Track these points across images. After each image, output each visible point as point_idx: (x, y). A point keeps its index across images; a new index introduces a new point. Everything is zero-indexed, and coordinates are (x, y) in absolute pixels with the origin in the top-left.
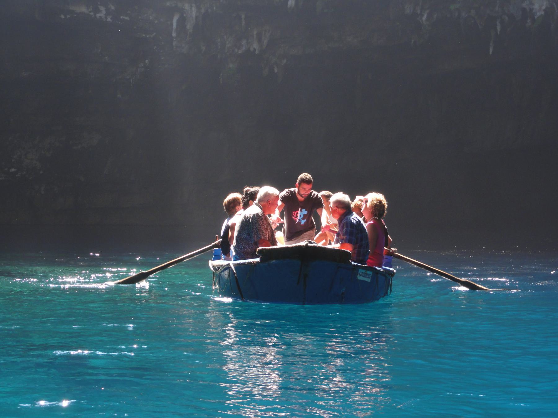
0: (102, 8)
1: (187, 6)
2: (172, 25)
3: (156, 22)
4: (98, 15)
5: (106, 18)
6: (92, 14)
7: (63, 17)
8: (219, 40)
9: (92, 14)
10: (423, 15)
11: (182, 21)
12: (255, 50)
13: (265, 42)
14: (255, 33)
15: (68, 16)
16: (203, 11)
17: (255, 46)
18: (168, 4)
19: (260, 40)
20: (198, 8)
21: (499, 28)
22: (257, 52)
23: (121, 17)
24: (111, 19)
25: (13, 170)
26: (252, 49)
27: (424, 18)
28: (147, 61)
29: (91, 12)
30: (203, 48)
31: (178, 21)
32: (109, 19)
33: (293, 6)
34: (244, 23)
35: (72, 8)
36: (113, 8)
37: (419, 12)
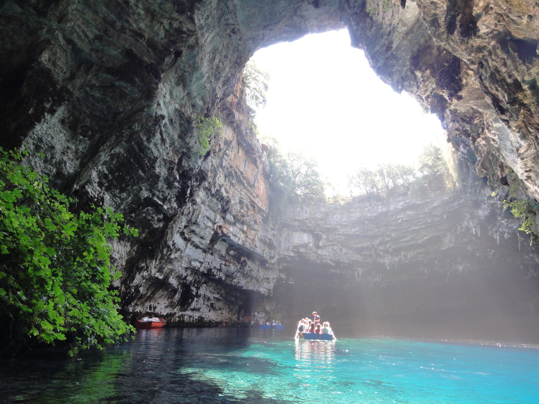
11: (358, 273)
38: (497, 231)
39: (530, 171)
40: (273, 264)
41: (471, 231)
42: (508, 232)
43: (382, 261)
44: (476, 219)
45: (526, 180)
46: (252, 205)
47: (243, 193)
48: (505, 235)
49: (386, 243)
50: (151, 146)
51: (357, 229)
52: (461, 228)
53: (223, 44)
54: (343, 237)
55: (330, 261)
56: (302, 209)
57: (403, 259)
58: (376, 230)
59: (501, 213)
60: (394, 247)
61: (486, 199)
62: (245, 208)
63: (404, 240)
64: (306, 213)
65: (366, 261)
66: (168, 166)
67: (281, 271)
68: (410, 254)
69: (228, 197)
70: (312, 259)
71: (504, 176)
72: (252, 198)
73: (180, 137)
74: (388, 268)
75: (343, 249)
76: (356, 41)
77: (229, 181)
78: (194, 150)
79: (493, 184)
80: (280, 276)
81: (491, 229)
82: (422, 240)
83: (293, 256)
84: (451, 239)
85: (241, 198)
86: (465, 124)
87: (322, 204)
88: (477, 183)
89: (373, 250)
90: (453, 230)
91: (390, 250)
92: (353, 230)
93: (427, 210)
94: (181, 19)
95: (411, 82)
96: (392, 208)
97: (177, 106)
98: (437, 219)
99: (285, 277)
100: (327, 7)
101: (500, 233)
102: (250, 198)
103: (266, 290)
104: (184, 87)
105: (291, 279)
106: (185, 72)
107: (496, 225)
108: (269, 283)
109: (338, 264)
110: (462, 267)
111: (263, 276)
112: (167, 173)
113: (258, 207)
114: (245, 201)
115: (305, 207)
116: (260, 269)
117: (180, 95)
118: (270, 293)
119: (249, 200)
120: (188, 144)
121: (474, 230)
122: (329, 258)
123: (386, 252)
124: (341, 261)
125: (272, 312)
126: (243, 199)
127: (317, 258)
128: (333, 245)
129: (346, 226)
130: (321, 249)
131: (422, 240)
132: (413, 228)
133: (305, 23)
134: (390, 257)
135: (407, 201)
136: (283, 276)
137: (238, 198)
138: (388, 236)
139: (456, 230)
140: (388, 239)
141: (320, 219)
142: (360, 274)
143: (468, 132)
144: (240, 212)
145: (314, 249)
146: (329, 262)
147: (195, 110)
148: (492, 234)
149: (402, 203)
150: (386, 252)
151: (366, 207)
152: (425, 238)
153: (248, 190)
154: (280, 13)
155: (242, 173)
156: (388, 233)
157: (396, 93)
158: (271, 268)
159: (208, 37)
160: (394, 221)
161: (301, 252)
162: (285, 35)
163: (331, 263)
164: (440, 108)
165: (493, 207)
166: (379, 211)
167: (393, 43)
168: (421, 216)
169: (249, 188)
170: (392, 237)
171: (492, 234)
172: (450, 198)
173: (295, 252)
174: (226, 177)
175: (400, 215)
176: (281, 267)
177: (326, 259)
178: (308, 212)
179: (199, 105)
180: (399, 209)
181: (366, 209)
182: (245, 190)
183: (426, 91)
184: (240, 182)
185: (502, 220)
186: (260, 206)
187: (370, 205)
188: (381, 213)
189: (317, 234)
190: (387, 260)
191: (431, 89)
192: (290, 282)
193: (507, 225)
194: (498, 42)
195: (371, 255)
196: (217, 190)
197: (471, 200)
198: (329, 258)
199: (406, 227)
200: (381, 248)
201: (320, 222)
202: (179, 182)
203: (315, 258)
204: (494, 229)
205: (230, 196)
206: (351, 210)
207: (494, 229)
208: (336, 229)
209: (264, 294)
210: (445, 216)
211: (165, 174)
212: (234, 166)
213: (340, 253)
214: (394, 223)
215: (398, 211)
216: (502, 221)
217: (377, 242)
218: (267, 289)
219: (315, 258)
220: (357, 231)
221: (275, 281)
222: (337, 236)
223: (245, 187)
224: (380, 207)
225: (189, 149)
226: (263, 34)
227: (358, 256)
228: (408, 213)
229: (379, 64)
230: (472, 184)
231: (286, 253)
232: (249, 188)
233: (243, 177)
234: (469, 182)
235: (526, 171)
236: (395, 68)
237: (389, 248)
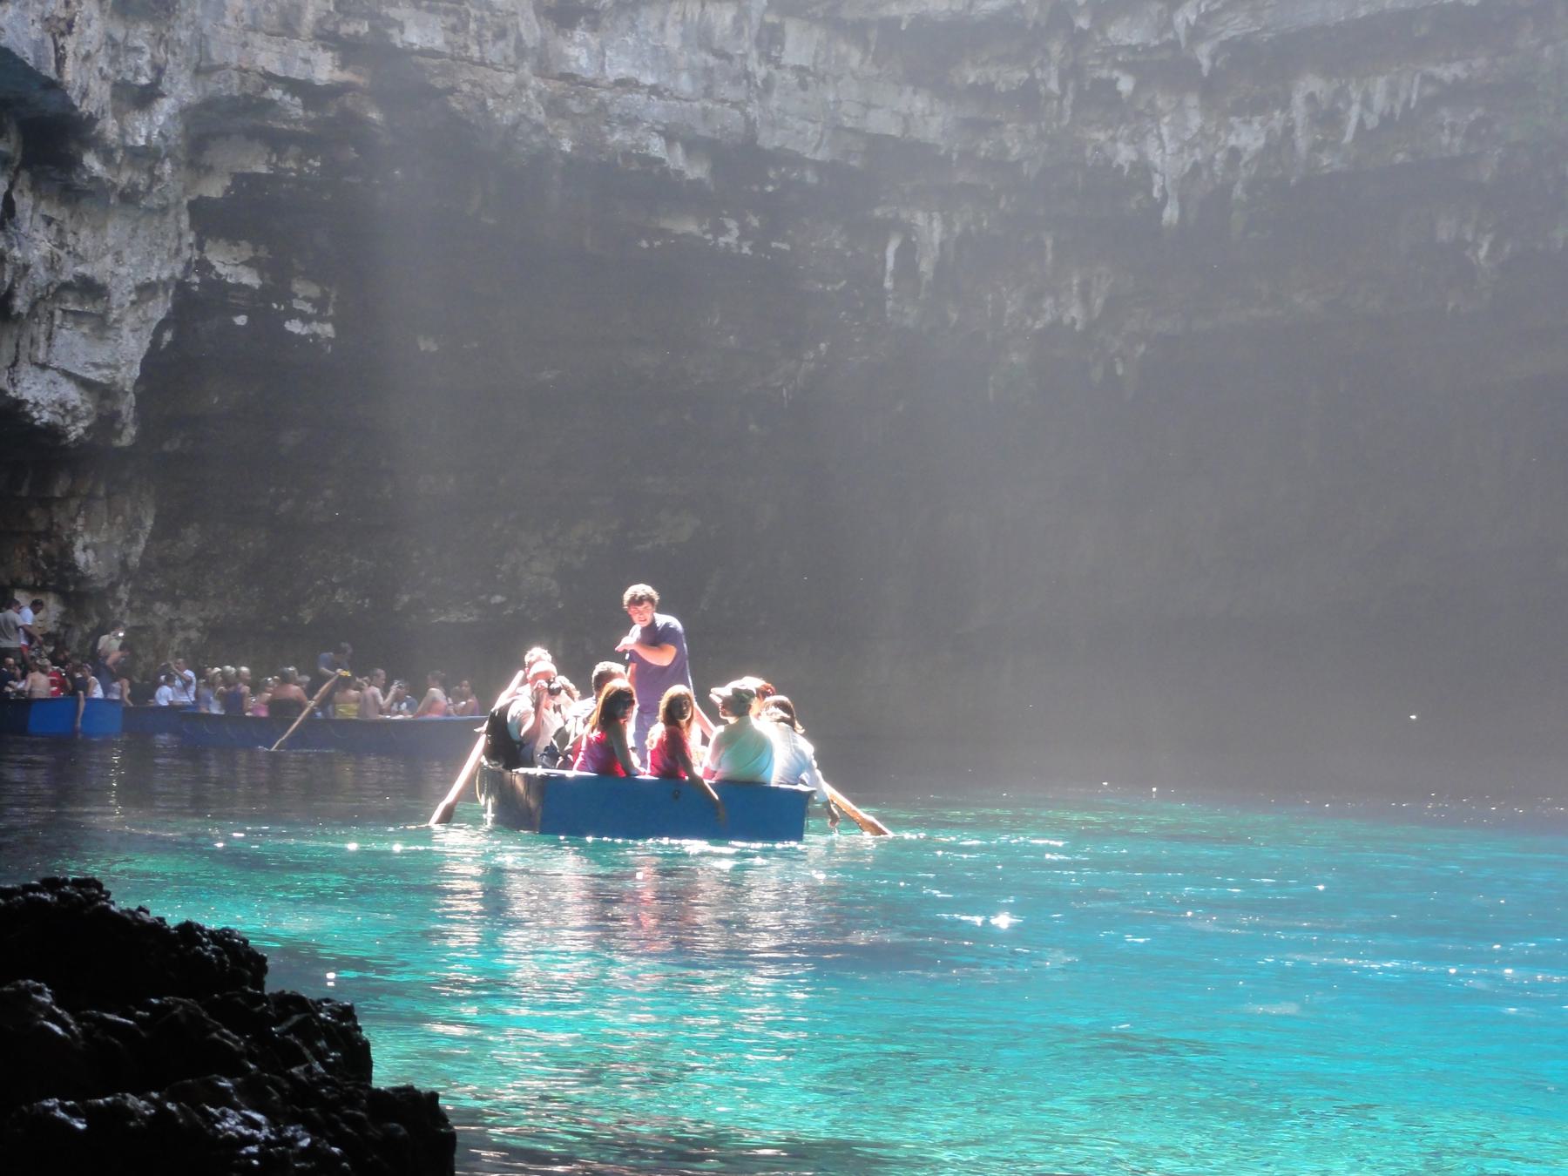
0: (732, 224)
1: (920, 218)
2: (884, 261)
3: (849, 254)
4: (722, 240)
5: (740, 248)
6: (709, 237)
7: (644, 244)
8: (990, 297)
9: (709, 237)
10: (1480, 246)
11: (908, 252)
12: (1074, 321)
13: (1099, 302)
14: (1075, 281)
15: (657, 243)
16: (957, 229)
17: (1075, 312)
18: (878, 212)
19: (1085, 298)
20: (948, 223)
22: (1078, 327)
23: (774, 244)
24: (751, 248)
25: (498, 599)
26: (1067, 320)
27: (1482, 253)
28: (823, 346)
29: (705, 233)
30: (954, 316)
31: (898, 254)
32: (746, 250)
33: (1175, 222)
34: (1050, 257)
35: (666, 224)
36: (755, 222)
37: (1469, 237)
40: (146, 157)
43: (1125, 154)
55: (669, 136)
57: (1302, 143)
60: (1236, 25)
65: (985, 147)
67: (210, 221)
68: (1374, 96)
70: (507, 116)
74: (1171, 213)
75: (792, 29)
80: (204, 266)
83: (334, 91)
89: (1056, 48)
91: (1203, 53)
99: (250, 278)
103: (73, 395)
105: (304, 291)
108: (102, 326)
109: (740, 162)
111: (52, 264)
116: (24, 202)
118: (107, 422)
122: (657, 108)
124: (769, 140)
125: (123, 593)
127: (555, 106)
130: (594, 26)
134: (1195, 121)
136: (232, 266)
142: (926, 266)
145: (531, 29)
146: (657, 147)
150: (1167, 69)
158: (129, 197)
161: (408, 52)
163: (677, 159)
173: (348, 51)
176: (214, 188)
177: (630, 122)
190: (1168, 147)
192: (294, 327)
195: (1028, 99)
198: (657, 108)
203: (538, 114)
209: (53, 433)
218: (85, 384)
219: (538, 114)
221: (159, 309)
227: (920, 103)
231: (268, 58)
237: (1196, 34)
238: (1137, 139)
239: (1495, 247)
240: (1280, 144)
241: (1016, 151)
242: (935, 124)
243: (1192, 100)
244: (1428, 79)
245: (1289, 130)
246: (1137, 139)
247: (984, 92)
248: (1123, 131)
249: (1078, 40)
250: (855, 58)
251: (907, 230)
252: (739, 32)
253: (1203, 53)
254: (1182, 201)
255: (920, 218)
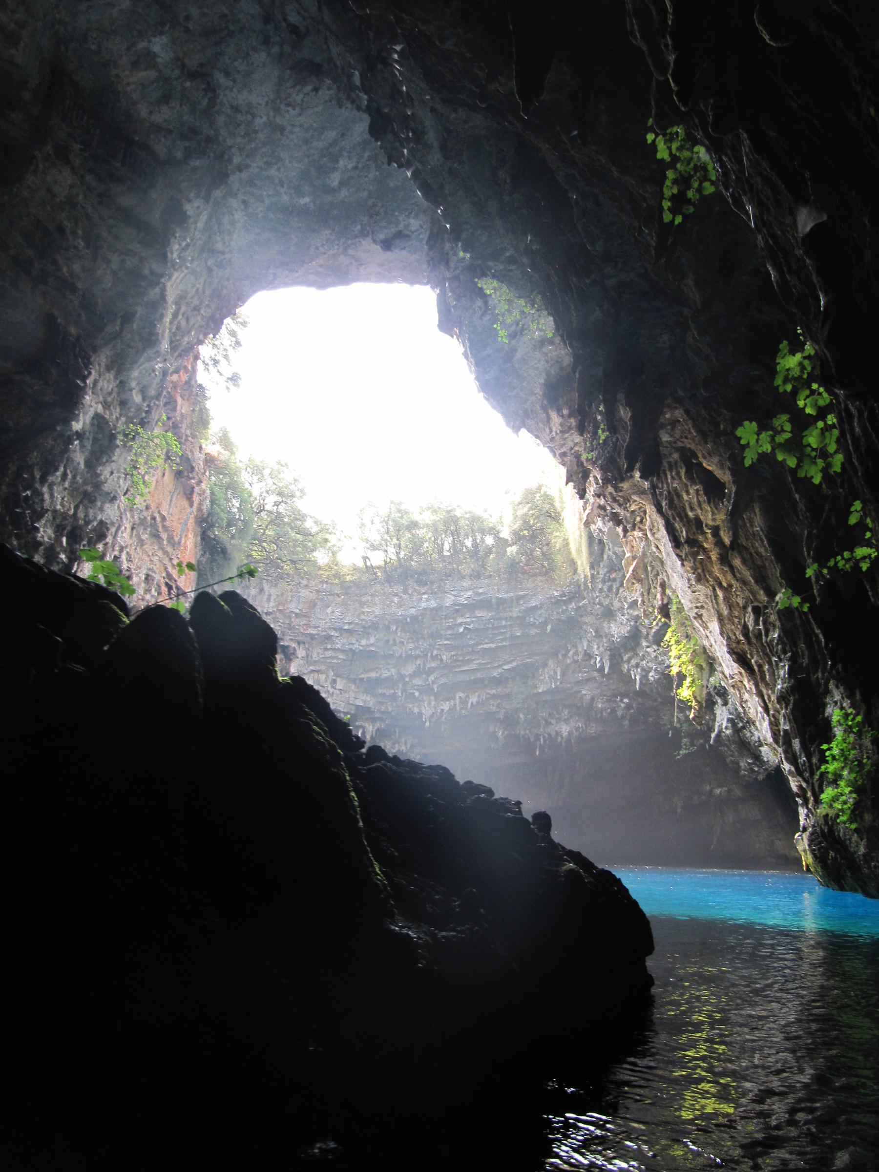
1: (367, 725)
13: (409, 746)
21: (542, 740)
38: (637, 666)
39: (702, 607)
41: (592, 661)
42: (656, 670)
43: (416, 710)
44: (605, 640)
45: (695, 618)
46: (167, 584)
47: (155, 559)
48: (651, 674)
49: (431, 671)
50: (45, 489)
51: (372, 640)
52: (576, 653)
53: (198, 289)
54: (341, 656)
56: (262, 590)
57: (458, 708)
58: (411, 646)
59: (648, 634)
60: (442, 681)
61: (626, 606)
62: (153, 590)
63: (466, 668)
64: (269, 600)
65: (383, 708)
66: (58, 521)
68: (473, 699)
69: (129, 569)
71: (665, 602)
72: (170, 569)
73: (88, 464)
75: (338, 680)
76: (449, 321)
77: (138, 536)
78: (106, 488)
79: (648, 607)
81: (629, 661)
82: (500, 670)
84: (555, 673)
85: (149, 569)
86: (616, 506)
87: (304, 582)
88: (613, 576)
89: (400, 685)
90: (560, 657)
91: (435, 687)
92: (364, 642)
93: (515, 612)
94: (143, 254)
95: (540, 425)
96: (449, 601)
97: (100, 408)
98: (533, 632)
100: (404, 253)
101: (643, 669)
102: (166, 569)
104: (119, 372)
106: (130, 347)
107: (637, 655)
110: (568, 729)
112: (53, 536)
113: (178, 588)
114: (157, 577)
115: (266, 587)
117: (108, 387)
119: (164, 575)
120: (98, 476)
121: (598, 659)
123: (427, 690)
126: (154, 571)
128: (318, 671)
129: (350, 632)
131: (500, 670)
132: (485, 646)
133: (358, 268)
135: (481, 591)
137: (145, 572)
138: (434, 658)
139: (565, 656)
140: (433, 665)
141: (296, 614)
143: (618, 517)
144: (143, 599)
147: (124, 412)
148: (629, 670)
149: (470, 593)
151: (396, 595)
152: (506, 667)
153: (166, 553)
154: (317, 248)
155: (164, 518)
156: (435, 652)
157: (509, 431)
159: (177, 278)
160: (449, 628)
162: (312, 277)
164: (580, 475)
165: (636, 622)
166: (423, 605)
167: (516, 350)
168: (504, 623)
169: (169, 549)
170: (442, 660)
171: (629, 670)
172: (561, 596)
174: (133, 529)
175: (462, 616)
178: (272, 598)
179: (134, 402)
180: (463, 605)
181: (396, 600)
182: (160, 553)
183: (562, 445)
184: (156, 536)
185: (648, 647)
186: (181, 585)
187: (405, 591)
188: (424, 609)
189: (288, 647)
191: (571, 444)
193: (656, 657)
194: (681, 457)
195: (394, 697)
196: (115, 556)
197: (600, 604)
199: (472, 642)
200: (417, 682)
201: (296, 621)
202: (65, 552)
204: (633, 662)
205: (133, 567)
206: (364, 599)
207: (633, 662)
208: (329, 637)
210: (549, 628)
211: (50, 538)
212: (153, 507)
213: (331, 690)
214: (449, 632)
215: (459, 610)
216: (648, 650)
217: (410, 669)
220: (372, 645)
222: (329, 654)
223: (162, 548)
224: (426, 596)
225: (98, 486)
226: (275, 274)
227: (368, 698)
228: (479, 613)
229: (487, 377)
230: (605, 575)
232: (169, 549)
233: (164, 526)
234: (601, 572)
235: (697, 607)
236: (515, 391)
237: (434, 682)
238: (419, 706)
239: (503, 733)
240: (452, 709)
241: (390, 709)
242: (371, 702)
243: (432, 698)
244: (488, 693)
245: (455, 705)
246: (419, 706)
247: (383, 695)
248: (416, 705)
249: (405, 684)
250: (353, 687)
251: (364, 728)
252: (326, 681)
253: (435, 687)
254: (430, 721)
255: (367, 725)
